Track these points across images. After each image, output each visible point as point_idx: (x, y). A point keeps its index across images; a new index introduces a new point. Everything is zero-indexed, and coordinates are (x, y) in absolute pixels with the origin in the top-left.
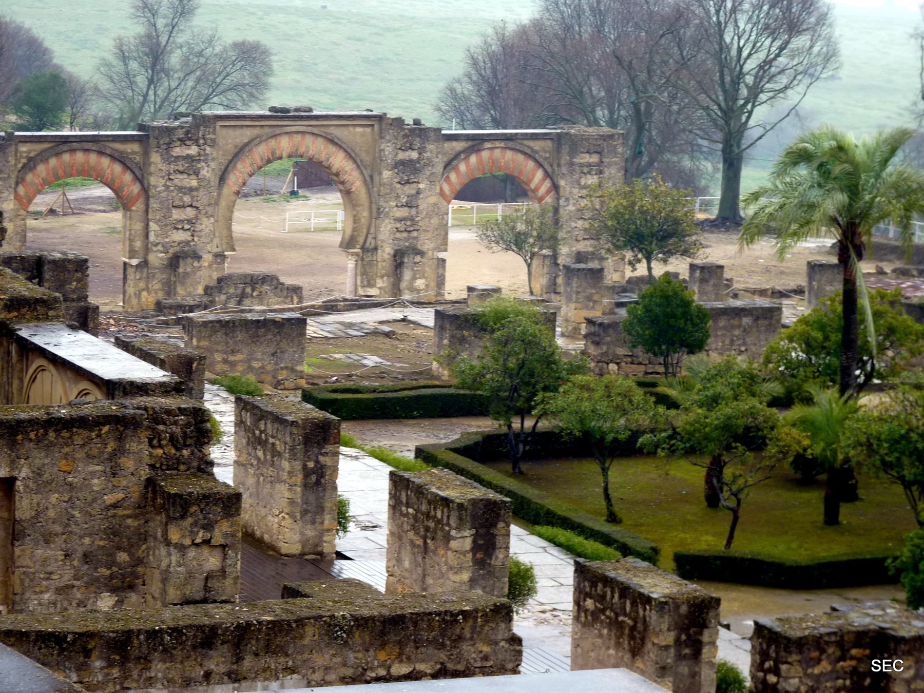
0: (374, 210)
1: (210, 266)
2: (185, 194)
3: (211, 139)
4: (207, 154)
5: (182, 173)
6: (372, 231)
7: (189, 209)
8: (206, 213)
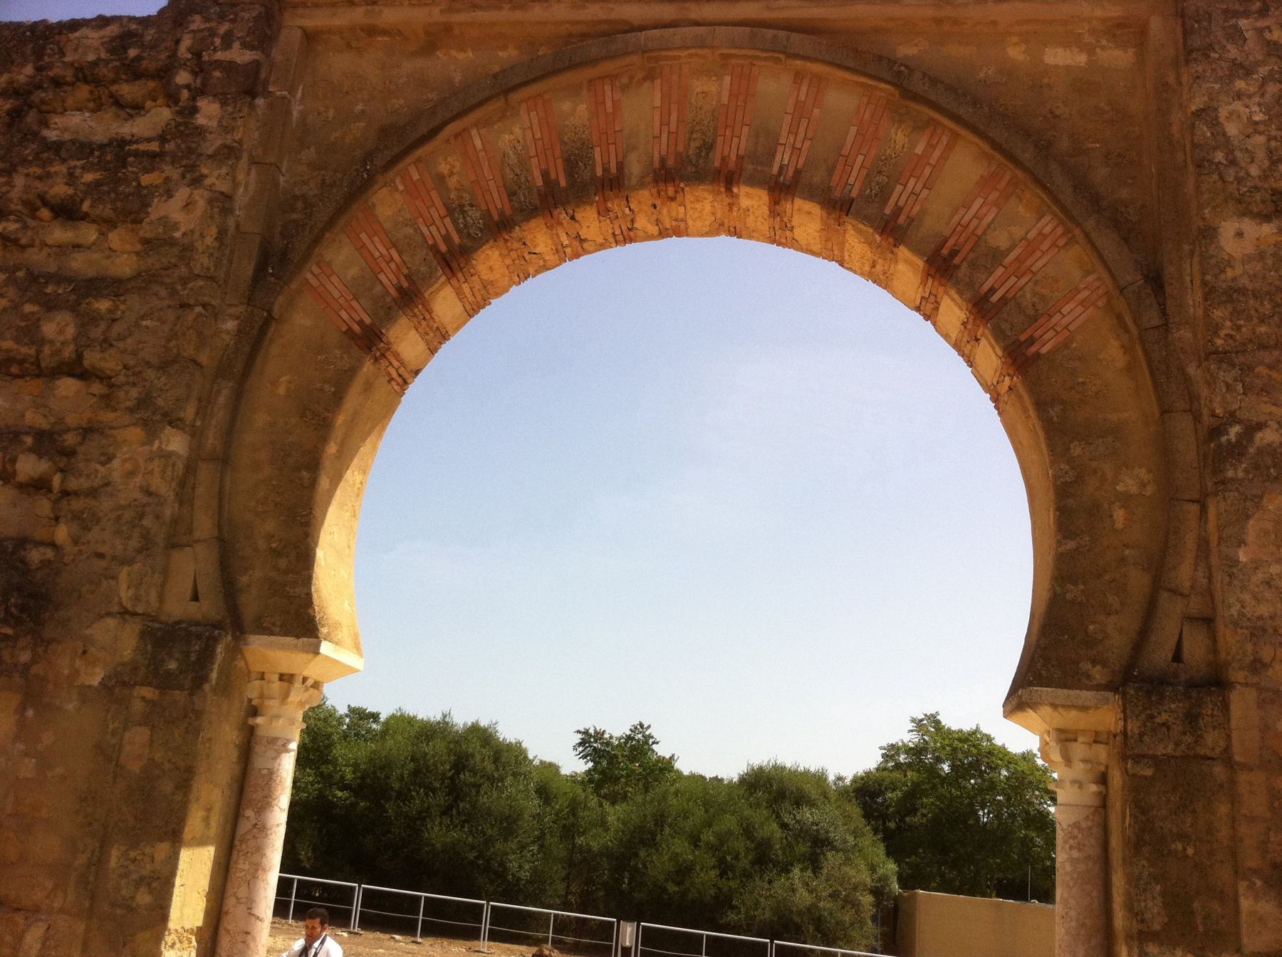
0: (1187, 448)
1: (117, 685)
2: (50, 306)
3: (229, 67)
4: (200, 131)
5: (67, 212)
6: (1185, 573)
7: (68, 386)
8: (143, 403)
